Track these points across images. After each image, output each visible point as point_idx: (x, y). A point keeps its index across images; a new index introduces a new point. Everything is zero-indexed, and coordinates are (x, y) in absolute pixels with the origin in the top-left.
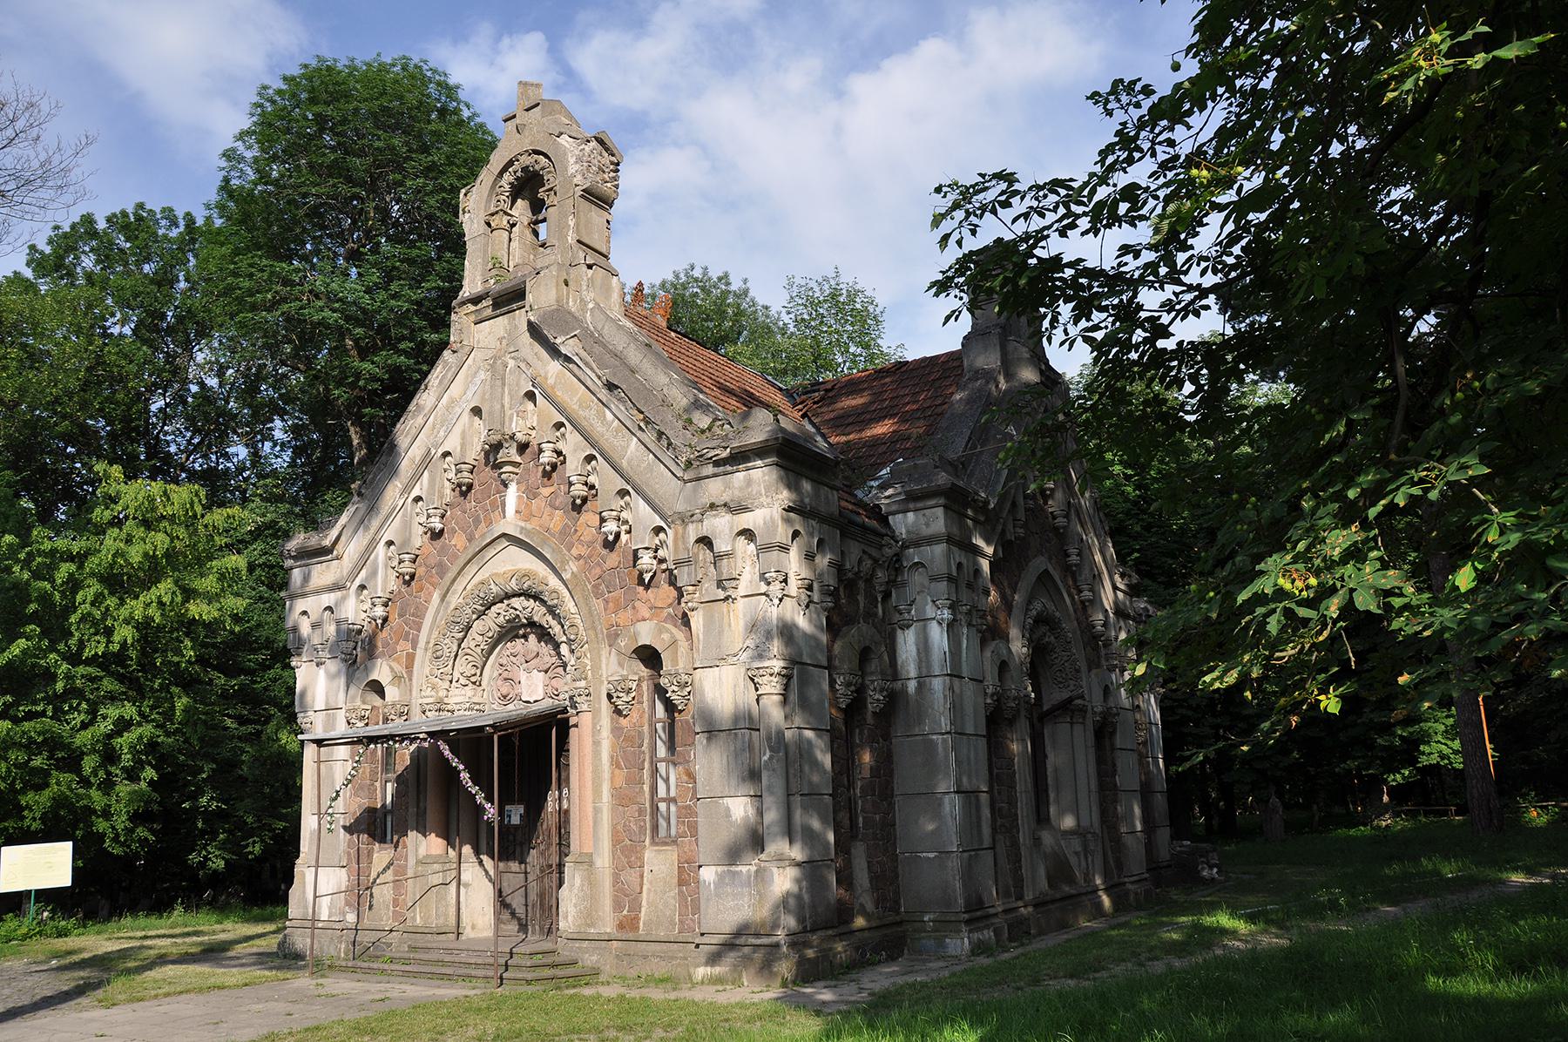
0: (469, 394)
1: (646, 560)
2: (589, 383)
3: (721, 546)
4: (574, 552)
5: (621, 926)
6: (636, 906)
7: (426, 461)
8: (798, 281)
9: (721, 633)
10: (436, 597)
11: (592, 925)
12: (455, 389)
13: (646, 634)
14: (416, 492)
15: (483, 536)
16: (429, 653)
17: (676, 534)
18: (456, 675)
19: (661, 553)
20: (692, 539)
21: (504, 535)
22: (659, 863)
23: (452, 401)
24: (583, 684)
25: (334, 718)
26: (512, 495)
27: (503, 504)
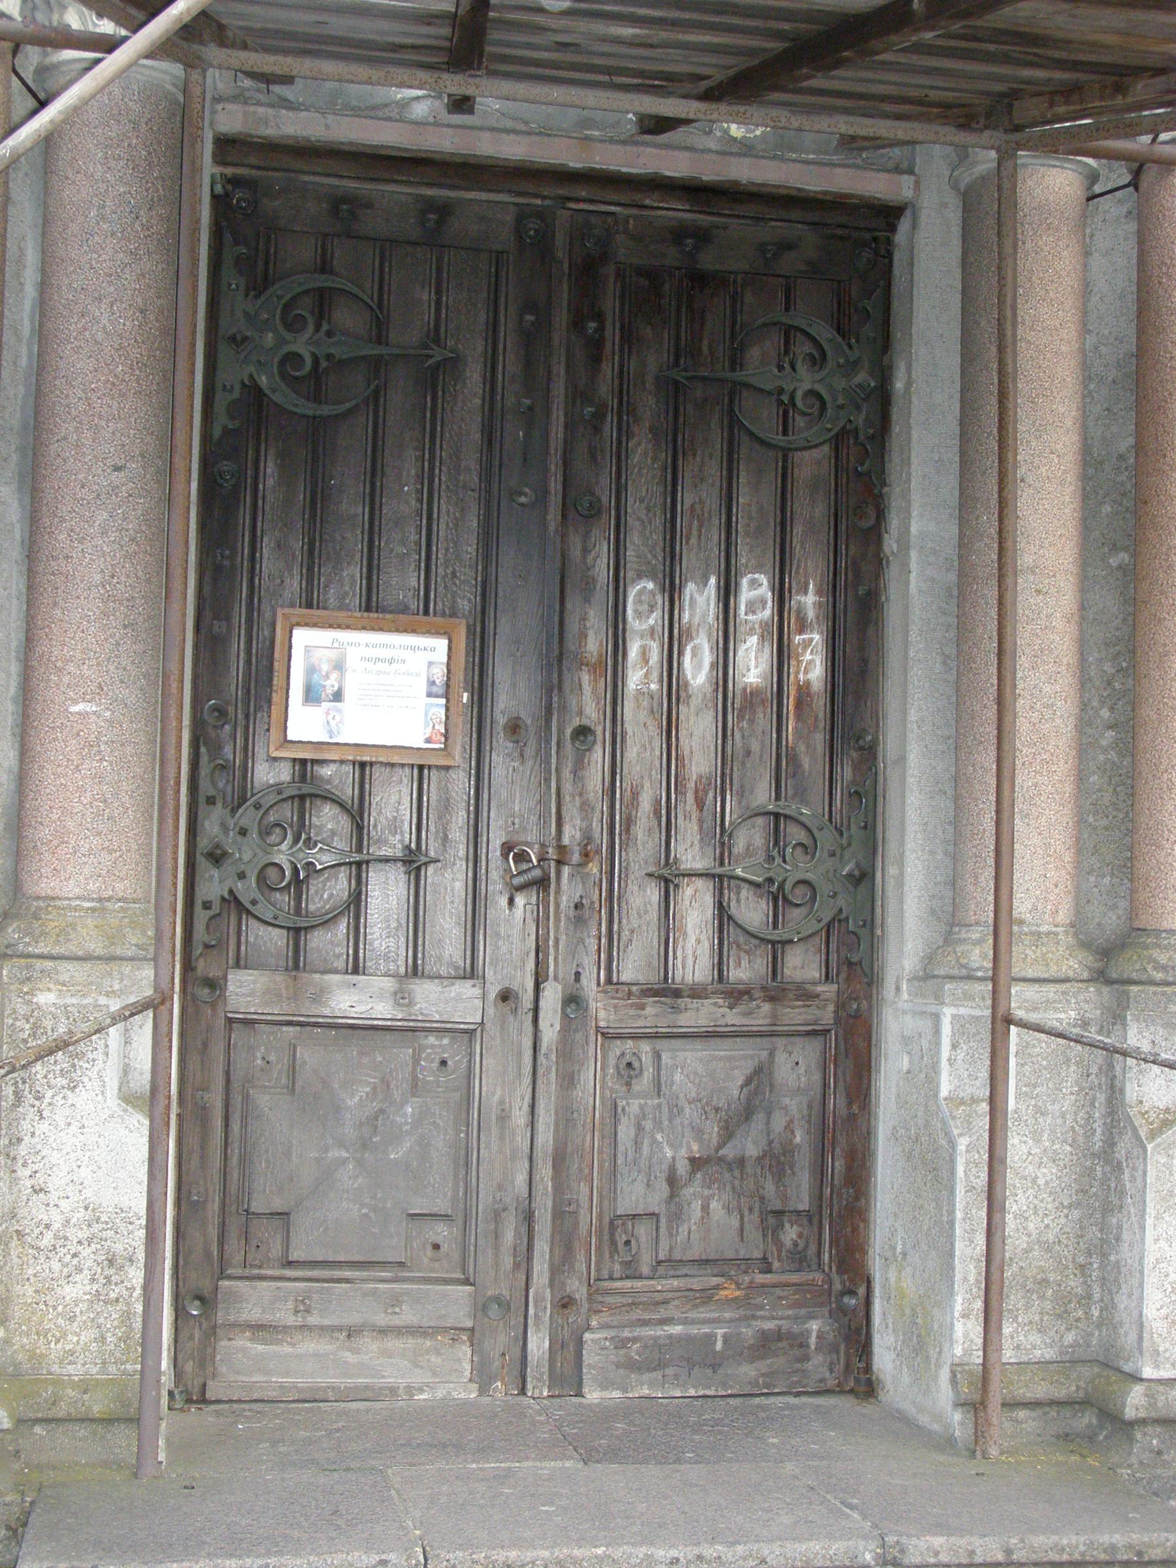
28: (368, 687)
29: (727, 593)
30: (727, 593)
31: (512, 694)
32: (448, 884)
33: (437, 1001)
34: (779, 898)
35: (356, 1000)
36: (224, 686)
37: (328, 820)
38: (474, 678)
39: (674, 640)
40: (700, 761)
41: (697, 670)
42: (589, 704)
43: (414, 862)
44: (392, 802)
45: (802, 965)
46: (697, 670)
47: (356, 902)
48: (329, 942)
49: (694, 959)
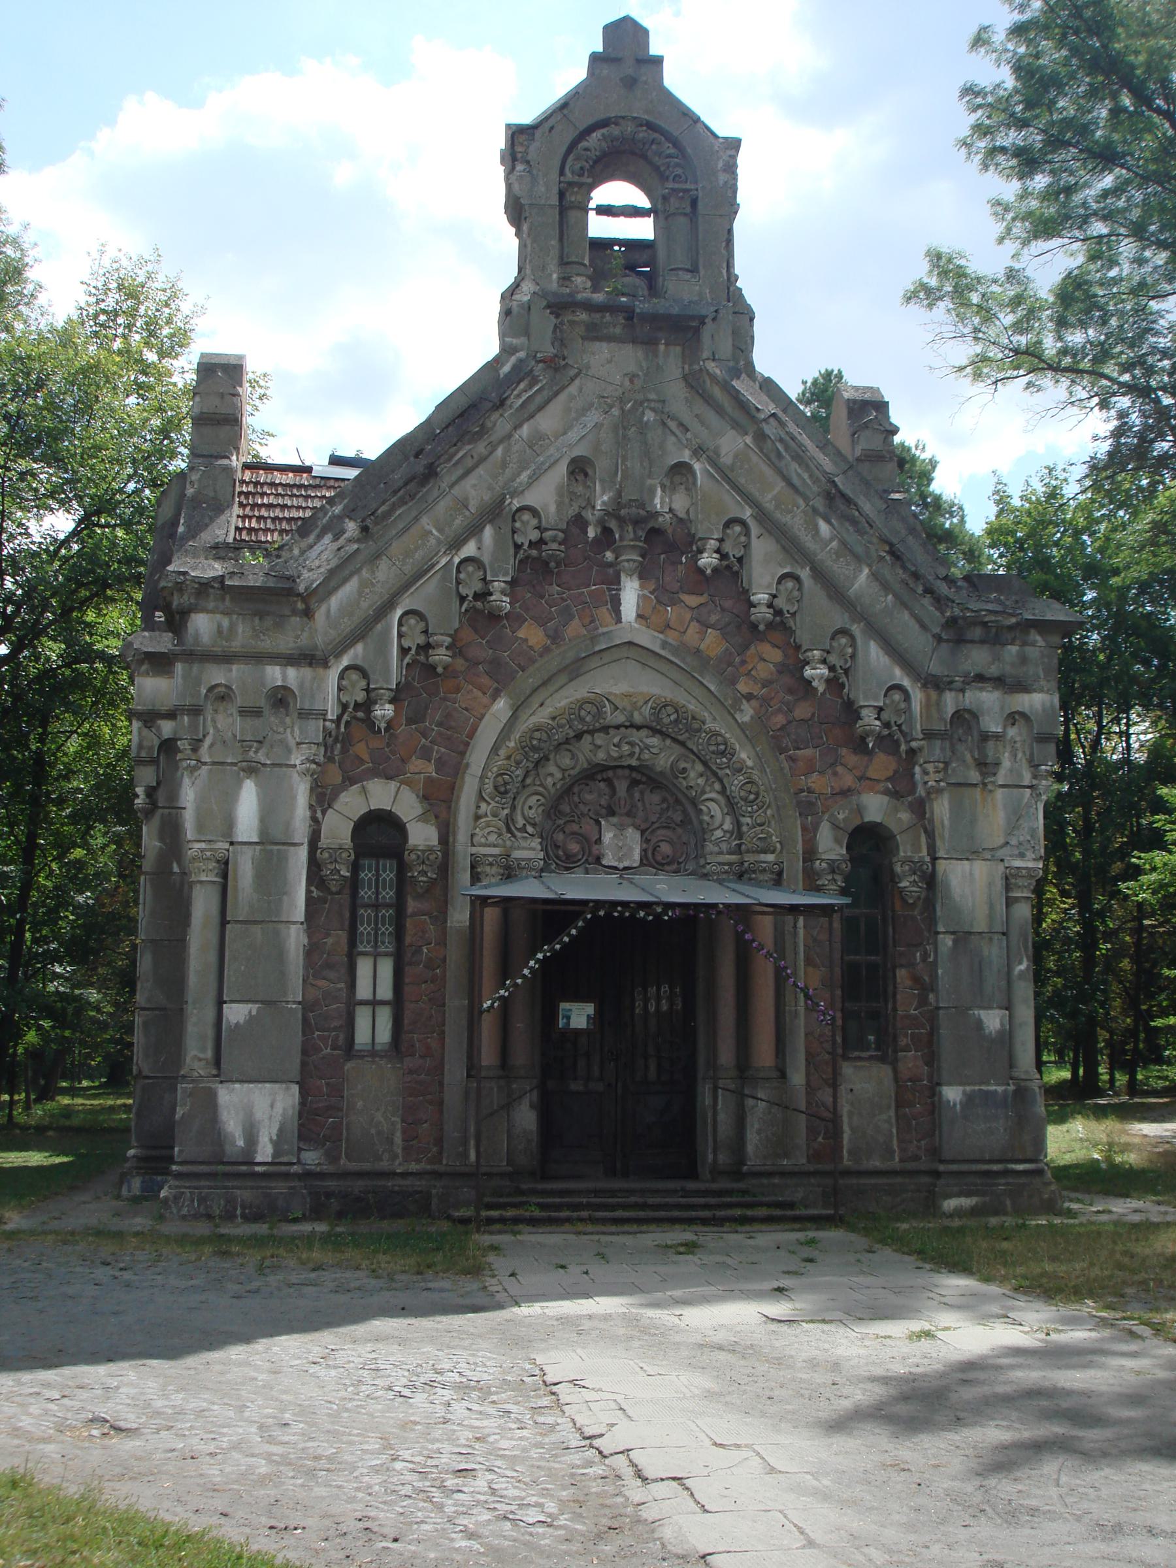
0: (573, 435)
1: (869, 719)
2: (796, 481)
4: (743, 687)
5: (815, 1156)
7: (494, 512)
10: (501, 706)
11: (786, 1155)
12: (547, 421)
13: (875, 807)
14: (469, 550)
15: (594, 639)
16: (489, 787)
17: (928, 698)
18: (520, 822)
19: (885, 716)
20: (950, 710)
21: (630, 643)
22: (865, 1083)
24: (770, 858)
25: (282, 859)
26: (631, 595)
27: (616, 603)
28: (578, 1015)
29: (658, 989)
30: (658, 989)
35: (575, 1086)
39: (646, 1001)
41: (652, 1009)
46: (652, 1009)
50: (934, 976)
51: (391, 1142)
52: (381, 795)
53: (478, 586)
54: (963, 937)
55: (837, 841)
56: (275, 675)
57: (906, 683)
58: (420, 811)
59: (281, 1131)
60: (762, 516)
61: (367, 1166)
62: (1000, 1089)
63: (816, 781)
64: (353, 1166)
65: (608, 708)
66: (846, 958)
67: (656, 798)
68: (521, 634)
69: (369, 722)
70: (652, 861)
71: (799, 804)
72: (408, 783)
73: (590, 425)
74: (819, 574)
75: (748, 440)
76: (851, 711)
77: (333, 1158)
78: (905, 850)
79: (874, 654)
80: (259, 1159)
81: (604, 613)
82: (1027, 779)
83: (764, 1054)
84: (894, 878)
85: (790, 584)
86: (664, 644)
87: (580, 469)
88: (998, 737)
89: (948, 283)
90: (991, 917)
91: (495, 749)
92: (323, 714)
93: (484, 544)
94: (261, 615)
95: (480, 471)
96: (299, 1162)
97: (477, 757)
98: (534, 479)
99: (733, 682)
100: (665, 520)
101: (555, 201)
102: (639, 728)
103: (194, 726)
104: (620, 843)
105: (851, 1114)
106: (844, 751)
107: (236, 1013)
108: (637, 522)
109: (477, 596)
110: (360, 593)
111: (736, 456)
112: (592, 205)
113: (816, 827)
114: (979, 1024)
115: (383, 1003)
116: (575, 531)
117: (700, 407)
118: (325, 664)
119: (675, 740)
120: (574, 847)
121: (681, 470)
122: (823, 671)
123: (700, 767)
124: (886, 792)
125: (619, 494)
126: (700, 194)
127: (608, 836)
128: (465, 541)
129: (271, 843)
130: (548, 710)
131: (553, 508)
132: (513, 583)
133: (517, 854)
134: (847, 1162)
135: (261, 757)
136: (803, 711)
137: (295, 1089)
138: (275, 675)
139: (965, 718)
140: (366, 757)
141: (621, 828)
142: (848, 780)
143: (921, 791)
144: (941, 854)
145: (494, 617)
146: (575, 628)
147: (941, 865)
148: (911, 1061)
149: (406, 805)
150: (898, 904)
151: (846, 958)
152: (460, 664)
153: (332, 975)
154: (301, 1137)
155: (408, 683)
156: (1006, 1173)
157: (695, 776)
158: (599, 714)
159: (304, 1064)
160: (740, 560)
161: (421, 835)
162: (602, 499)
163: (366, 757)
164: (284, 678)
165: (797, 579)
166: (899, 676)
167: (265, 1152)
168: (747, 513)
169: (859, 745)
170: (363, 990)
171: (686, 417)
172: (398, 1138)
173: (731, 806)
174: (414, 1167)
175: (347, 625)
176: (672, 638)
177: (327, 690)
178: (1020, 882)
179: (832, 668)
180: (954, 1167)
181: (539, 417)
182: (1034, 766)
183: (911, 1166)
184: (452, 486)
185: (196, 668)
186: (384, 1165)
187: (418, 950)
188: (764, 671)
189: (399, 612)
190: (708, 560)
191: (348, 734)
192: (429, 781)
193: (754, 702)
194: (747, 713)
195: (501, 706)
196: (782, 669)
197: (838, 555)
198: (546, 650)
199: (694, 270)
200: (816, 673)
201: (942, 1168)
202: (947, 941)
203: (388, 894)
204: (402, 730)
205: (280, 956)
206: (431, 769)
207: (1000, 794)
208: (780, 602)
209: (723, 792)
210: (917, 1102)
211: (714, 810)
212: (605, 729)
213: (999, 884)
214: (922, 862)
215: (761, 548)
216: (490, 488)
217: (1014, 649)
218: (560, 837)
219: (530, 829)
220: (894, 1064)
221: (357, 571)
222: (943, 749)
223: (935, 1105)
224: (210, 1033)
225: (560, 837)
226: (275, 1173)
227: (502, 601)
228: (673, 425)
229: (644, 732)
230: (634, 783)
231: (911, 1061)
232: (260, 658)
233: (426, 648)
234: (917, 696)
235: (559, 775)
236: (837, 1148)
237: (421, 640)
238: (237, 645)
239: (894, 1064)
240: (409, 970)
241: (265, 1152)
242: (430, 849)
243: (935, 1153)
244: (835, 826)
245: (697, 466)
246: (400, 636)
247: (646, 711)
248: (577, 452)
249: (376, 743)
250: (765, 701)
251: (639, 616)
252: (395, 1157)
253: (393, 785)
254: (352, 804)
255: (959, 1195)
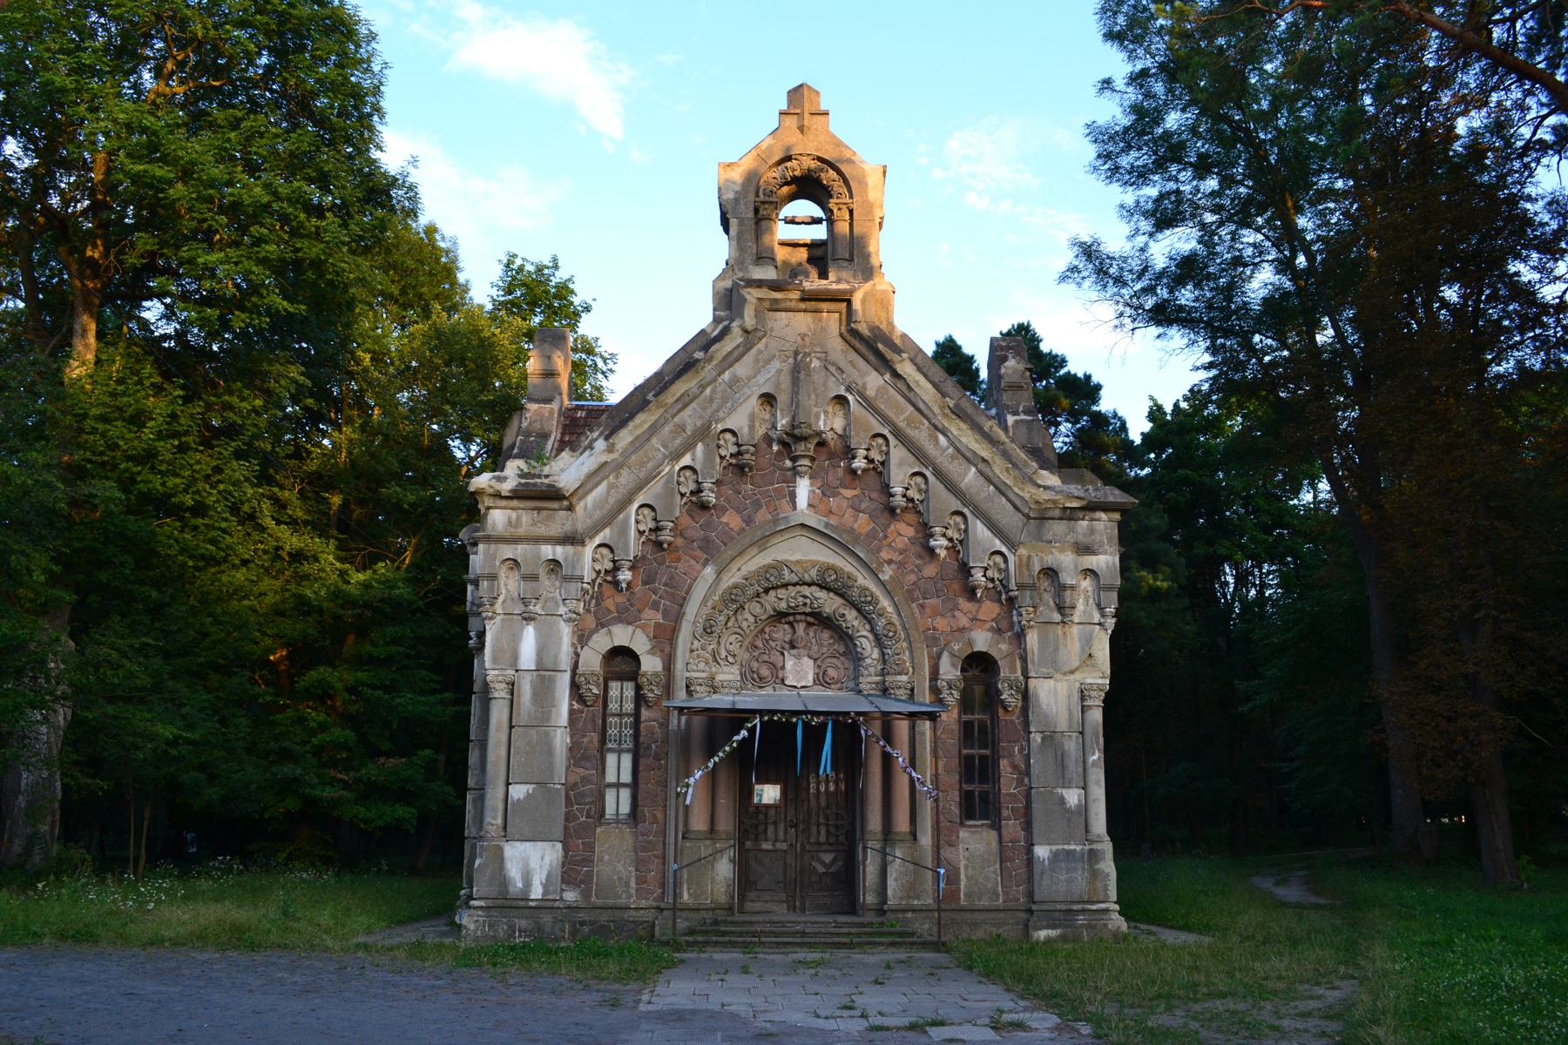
0: (761, 379)
1: (978, 576)
3: (1068, 578)
4: (885, 555)
6: (953, 879)
7: (703, 433)
8: (518, 262)
9: (1056, 650)
12: (741, 369)
13: (982, 641)
14: (686, 460)
15: (775, 521)
16: (700, 629)
18: (723, 653)
19: (989, 573)
20: (1037, 569)
21: (803, 525)
22: (974, 845)
23: (735, 380)
24: (904, 678)
25: (552, 681)
27: (793, 496)
28: (769, 794)
31: (791, 796)
32: (781, 827)
33: (779, 846)
34: (837, 827)
35: (766, 846)
36: (746, 793)
37: (761, 816)
38: (784, 792)
39: (818, 783)
40: (823, 804)
42: (803, 796)
43: (775, 823)
44: (772, 812)
45: (842, 839)
47: (765, 831)
48: (762, 836)
49: (823, 838)
50: (1028, 765)
51: (627, 885)
52: (622, 635)
53: (692, 486)
54: (1050, 738)
55: (953, 665)
56: (548, 551)
57: (1004, 549)
58: (649, 647)
59: (548, 876)
60: (898, 433)
61: (610, 902)
62: (1078, 848)
63: (942, 624)
64: (600, 902)
65: (786, 571)
66: (965, 752)
67: (826, 635)
68: (724, 519)
69: (616, 583)
70: (821, 680)
71: (926, 638)
72: (643, 627)
73: (773, 371)
74: (938, 474)
75: (887, 376)
76: (965, 570)
77: (586, 895)
78: (1004, 673)
79: (980, 530)
80: (533, 897)
81: (784, 503)
82: (1097, 618)
83: (902, 823)
84: (999, 693)
85: (919, 479)
86: (827, 525)
87: (768, 399)
88: (1073, 588)
89: (1094, 262)
90: (1070, 720)
91: (704, 602)
92: (581, 578)
93: (696, 456)
94: (539, 509)
95: (694, 405)
96: (562, 899)
97: (692, 609)
98: (733, 409)
99: (879, 550)
100: (830, 435)
101: (751, 215)
102: (809, 585)
103: (491, 588)
104: (800, 671)
105: (966, 867)
106: (961, 600)
107: (518, 792)
108: (804, 439)
109: (692, 493)
110: (608, 493)
111: (878, 390)
112: (781, 216)
113: (939, 656)
114: (1062, 800)
115: (625, 785)
116: (764, 446)
117: (853, 356)
118: (582, 543)
119: (836, 594)
120: (765, 672)
121: (841, 400)
122: (944, 542)
123: (854, 613)
124: (991, 629)
125: (793, 418)
126: (855, 206)
127: (789, 664)
128: (682, 455)
129: (545, 670)
130: (744, 571)
131: (746, 430)
132: (718, 483)
133: (720, 677)
134: (963, 901)
135: (538, 609)
136: (930, 570)
137: (559, 846)
138: (548, 551)
139: (1051, 573)
140: (613, 609)
141: (798, 657)
142: (964, 621)
143: (1017, 628)
144: (1032, 674)
145: (704, 507)
146: (763, 515)
147: (1032, 683)
148: (1012, 827)
149: (640, 643)
150: (1001, 711)
151: (965, 752)
152: (680, 541)
153: (588, 765)
154: (563, 881)
155: (643, 557)
156: (1083, 911)
157: (851, 618)
158: (781, 575)
159: (566, 828)
160: (882, 463)
161: (651, 664)
162: (783, 422)
163: (613, 609)
164: (554, 553)
165: (924, 476)
166: (999, 545)
167: (537, 892)
168: (886, 432)
169: (970, 592)
170: (611, 777)
171: (842, 364)
172: (633, 884)
173: (879, 641)
174: (644, 903)
175: (598, 514)
176: (833, 521)
177: (587, 560)
178: (1093, 694)
179: (951, 540)
180: (1044, 907)
181: (736, 366)
182: (1101, 608)
183: (1010, 904)
184: (674, 416)
185: (493, 547)
186: (623, 901)
187: (649, 747)
188: (901, 543)
189: (636, 505)
190: (859, 463)
191: (601, 593)
192: (657, 625)
193: (893, 566)
194: (887, 574)
195: (709, 571)
196: (912, 541)
197: (953, 458)
198: (743, 530)
199: (851, 260)
200: (939, 543)
201: (1034, 907)
202: (1037, 738)
203: (629, 707)
204: (638, 589)
205: (549, 750)
206: (659, 618)
207: (1075, 629)
208: (910, 493)
209: (872, 630)
210: (1017, 860)
211: (866, 645)
212: (785, 586)
213: (1076, 696)
214: (1017, 680)
215: (898, 453)
216: (701, 417)
217: (1084, 523)
218: (755, 665)
219: (730, 659)
220: (999, 830)
221: (607, 477)
222: (1032, 597)
223: (1030, 860)
224: (501, 806)
225: (755, 665)
226: (544, 906)
227: (710, 497)
228: (832, 369)
229: (814, 588)
230: (809, 624)
231: (1012, 827)
232: (538, 540)
233: (657, 529)
234: (1011, 558)
235: (752, 619)
236: (953, 894)
237: (652, 525)
238: (521, 531)
239: (999, 830)
240: (642, 761)
241: (537, 892)
242: (656, 674)
243: (1030, 895)
244: (952, 655)
245: (850, 398)
246: (637, 522)
247: (813, 573)
248: (764, 390)
249: (620, 599)
250: (901, 565)
251: (810, 505)
252: (630, 896)
253: (630, 628)
254: (601, 643)
255: (1047, 927)
